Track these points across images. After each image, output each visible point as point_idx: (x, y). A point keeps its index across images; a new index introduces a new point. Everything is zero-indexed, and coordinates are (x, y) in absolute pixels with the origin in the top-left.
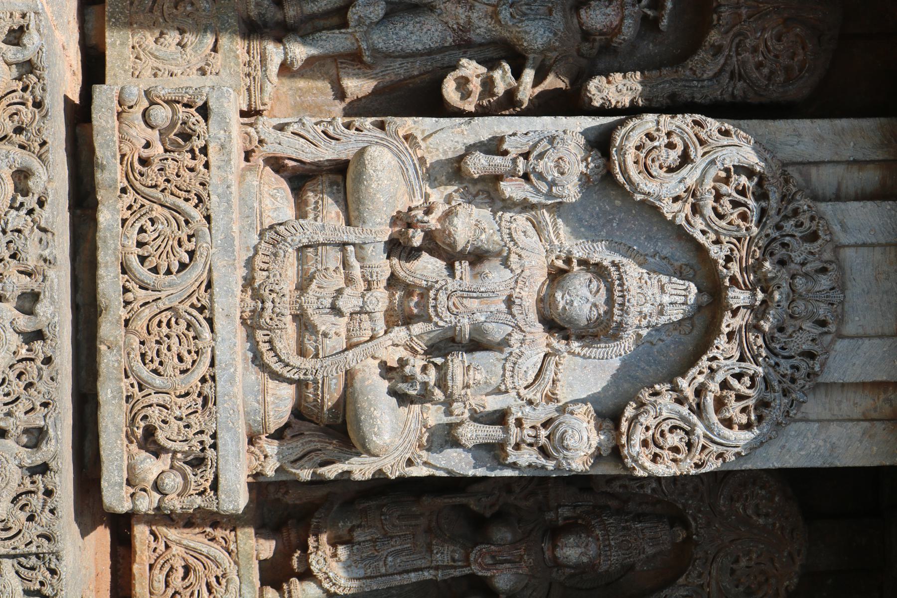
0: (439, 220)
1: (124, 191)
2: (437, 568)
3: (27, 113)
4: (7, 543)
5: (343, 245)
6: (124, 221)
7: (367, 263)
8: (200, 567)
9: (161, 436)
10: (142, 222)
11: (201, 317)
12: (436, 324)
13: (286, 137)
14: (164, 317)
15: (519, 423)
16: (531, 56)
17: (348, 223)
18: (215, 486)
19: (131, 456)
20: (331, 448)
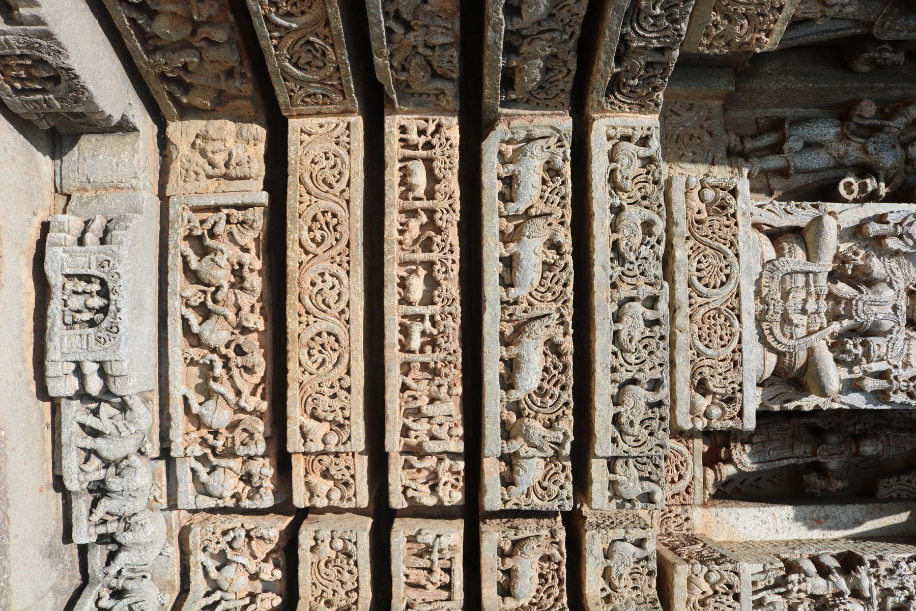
0: (862, 259)
1: (688, 238)
2: (798, 457)
3: (650, 188)
4: (638, 449)
5: (807, 273)
6: (689, 256)
7: (818, 284)
8: (673, 456)
9: (710, 385)
10: (699, 257)
11: (733, 314)
12: (856, 320)
13: (763, 211)
14: (712, 313)
15: (896, 378)
16: (881, 172)
17: (808, 260)
18: (741, 414)
19: (692, 397)
20: (792, 392)
